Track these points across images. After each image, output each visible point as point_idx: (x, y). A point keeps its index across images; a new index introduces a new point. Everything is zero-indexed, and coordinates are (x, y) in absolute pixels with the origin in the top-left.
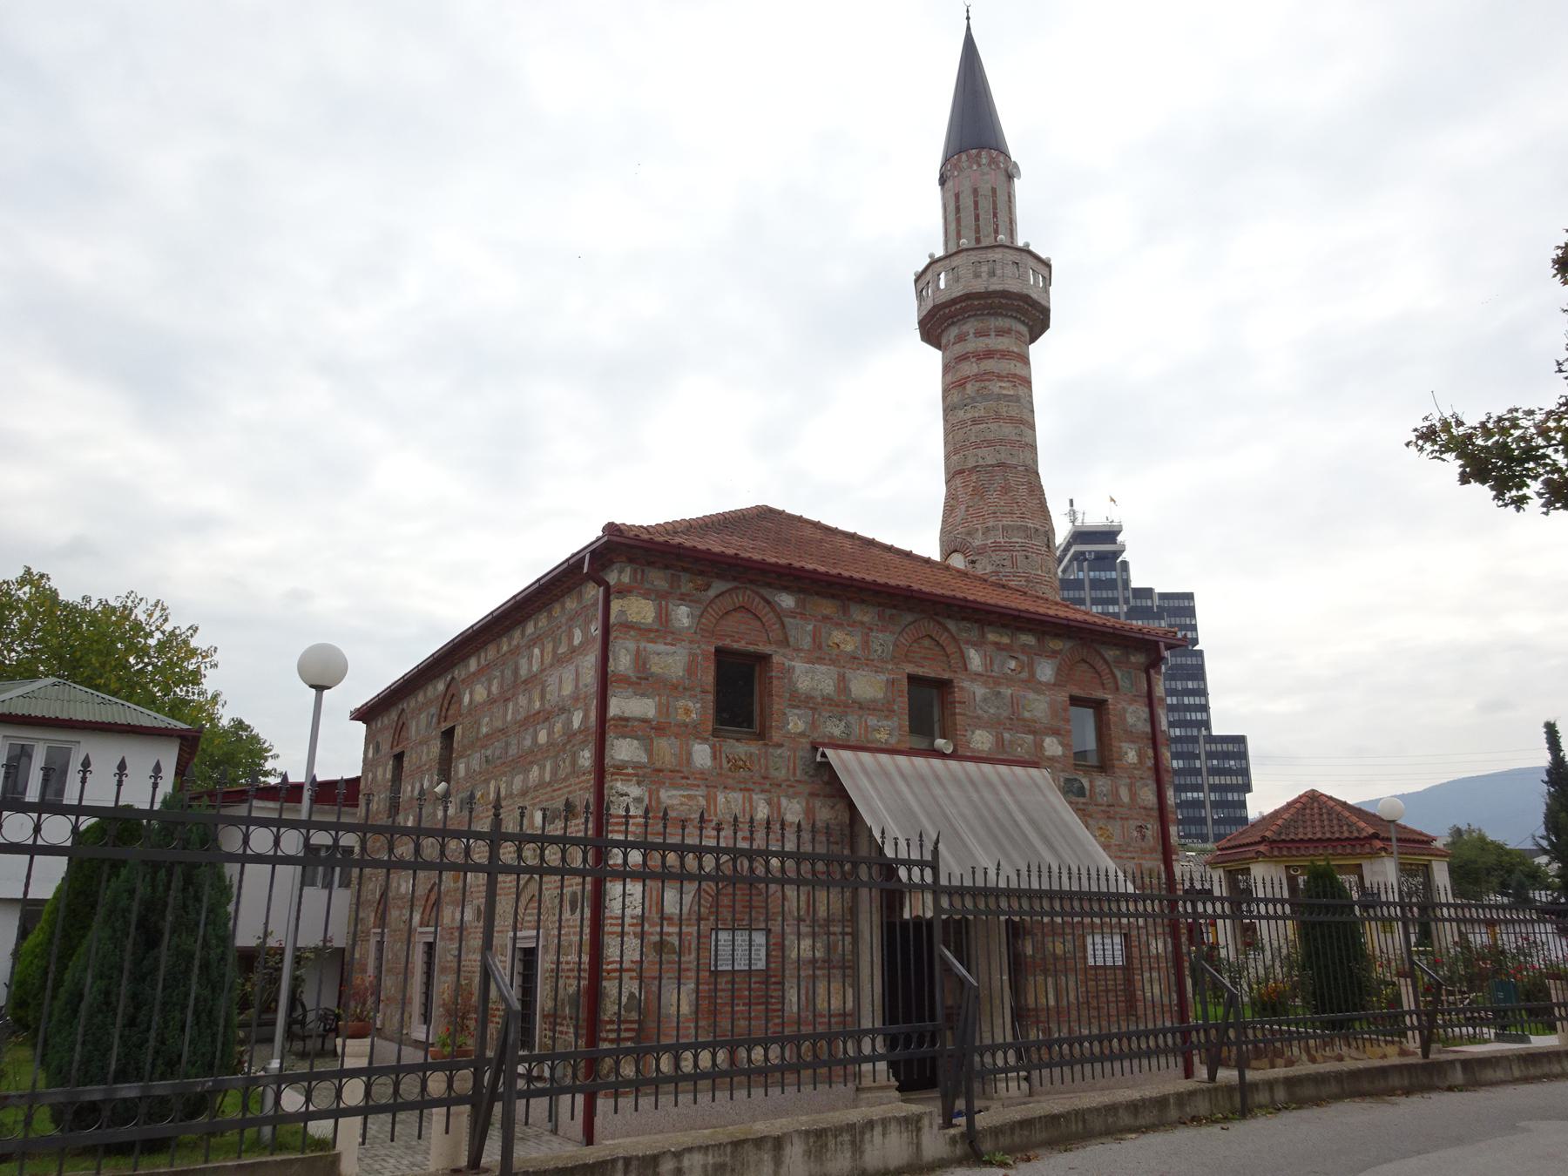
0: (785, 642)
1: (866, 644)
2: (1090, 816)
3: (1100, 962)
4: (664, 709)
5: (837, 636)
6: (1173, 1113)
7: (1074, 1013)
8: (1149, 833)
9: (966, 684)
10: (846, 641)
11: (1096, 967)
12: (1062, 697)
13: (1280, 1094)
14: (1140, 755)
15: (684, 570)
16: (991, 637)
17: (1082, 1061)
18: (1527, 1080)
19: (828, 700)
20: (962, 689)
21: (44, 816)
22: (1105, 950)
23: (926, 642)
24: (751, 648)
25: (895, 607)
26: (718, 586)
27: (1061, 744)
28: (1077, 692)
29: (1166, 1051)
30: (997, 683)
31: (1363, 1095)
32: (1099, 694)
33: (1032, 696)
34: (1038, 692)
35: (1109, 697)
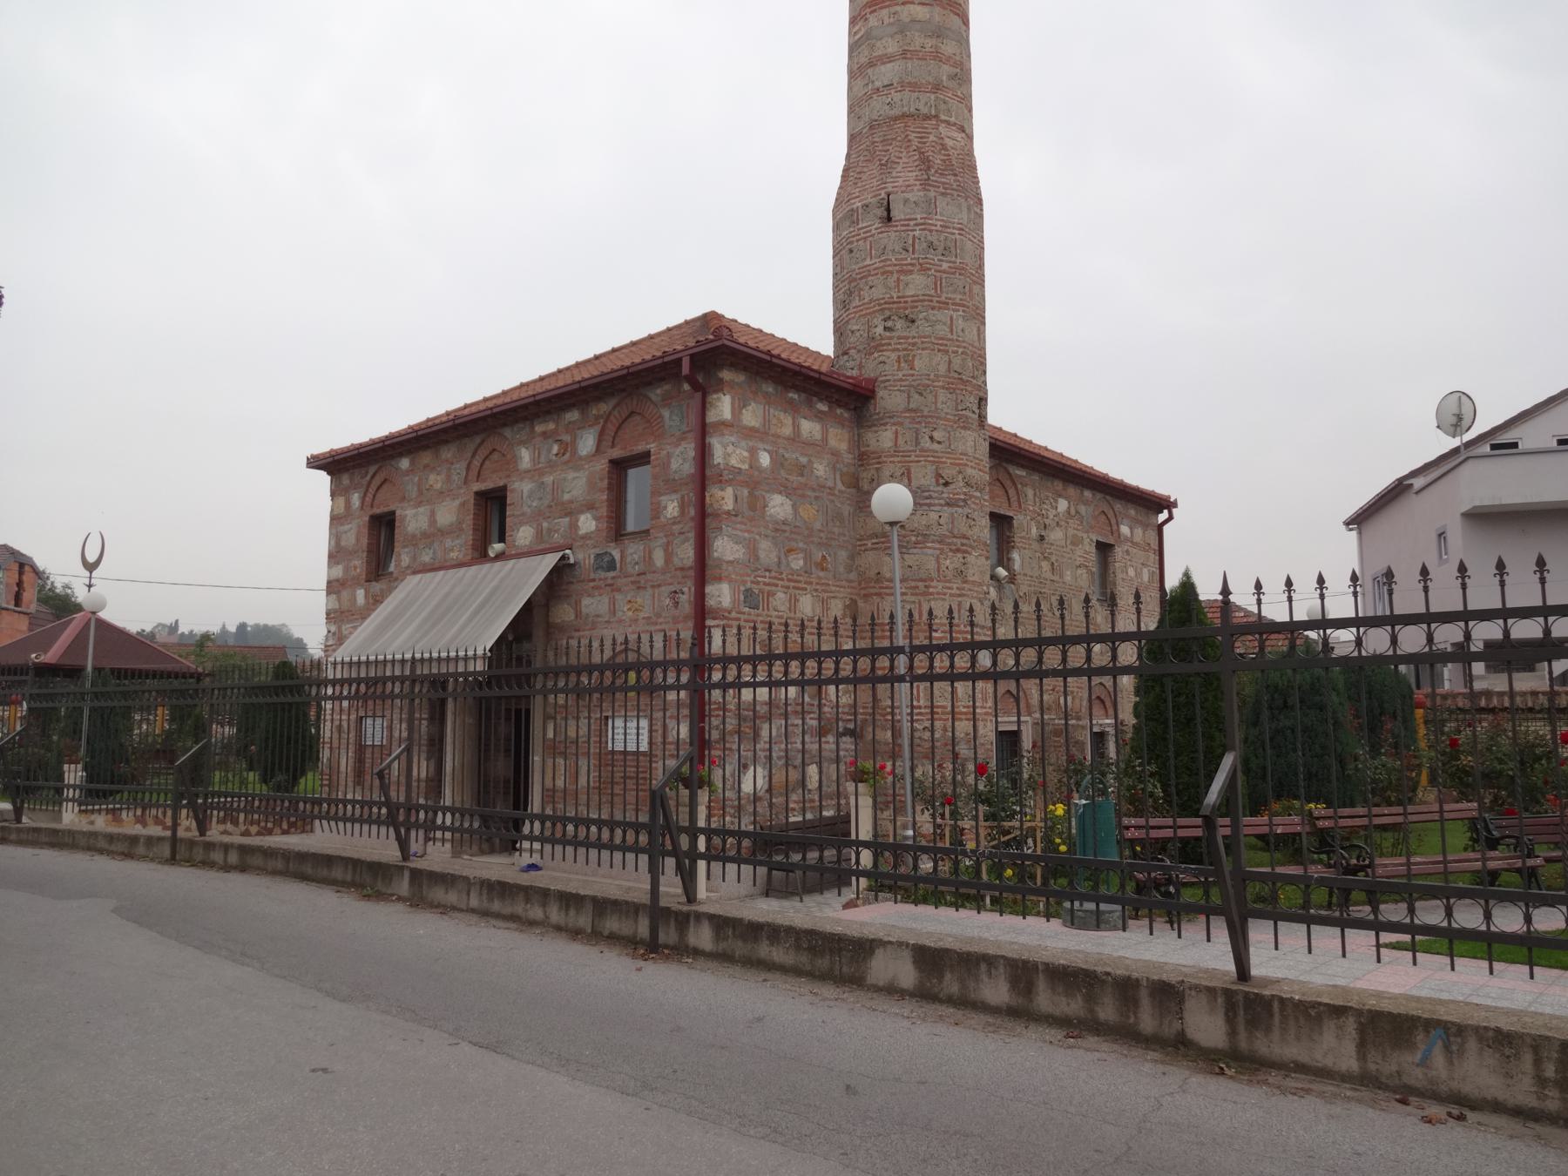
0: (403, 499)
1: (449, 477)
2: (619, 590)
3: (631, 747)
4: (346, 570)
5: (432, 477)
6: (141, 850)
7: (583, 798)
8: (684, 598)
9: (516, 485)
10: (436, 480)
11: (625, 753)
12: (601, 465)
13: (233, 858)
14: (682, 506)
15: (354, 467)
16: (539, 428)
17: (588, 845)
18: (485, 914)
19: (425, 535)
20: (513, 491)
21: (1397, 628)
22: (629, 733)
23: (495, 456)
24: (386, 510)
25: (466, 436)
26: (372, 469)
27: (595, 518)
28: (617, 453)
29: (637, 849)
30: (542, 474)
31: (303, 878)
32: (640, 448)
33: (571, 475)
34: (577, 468)
35: (652, 447)
